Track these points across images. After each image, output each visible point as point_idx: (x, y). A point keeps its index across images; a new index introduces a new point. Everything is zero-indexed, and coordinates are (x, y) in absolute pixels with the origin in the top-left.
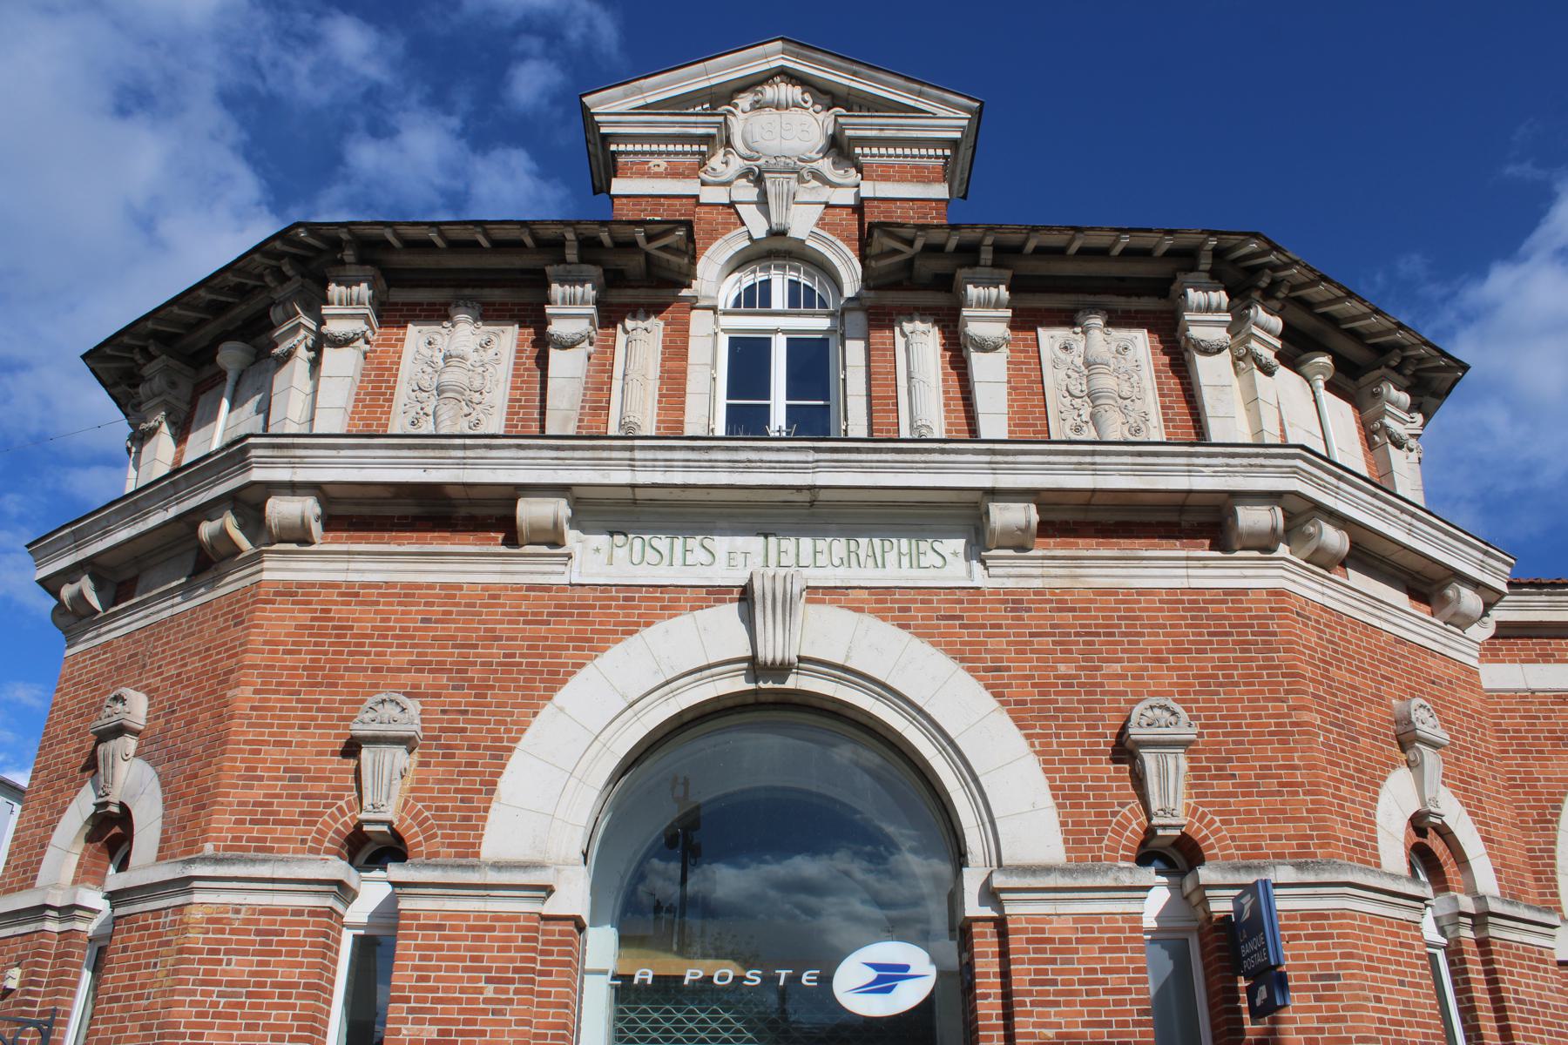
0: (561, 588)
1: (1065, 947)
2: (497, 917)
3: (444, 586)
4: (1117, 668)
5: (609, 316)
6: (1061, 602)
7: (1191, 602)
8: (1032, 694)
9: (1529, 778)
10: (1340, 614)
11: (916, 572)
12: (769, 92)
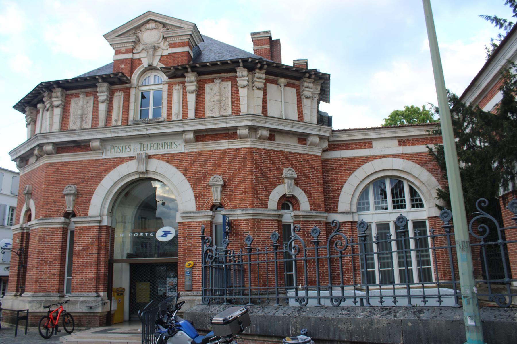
0: (102, 159)
1: (194, 228)
2: (92, 227)
3: (80, 161)
4: (211, 168)
6: (200, 154)
7: (228, 152)
9: (337, 179)
10: (269, 150)
11: (171, 150)
12: (148, 26)
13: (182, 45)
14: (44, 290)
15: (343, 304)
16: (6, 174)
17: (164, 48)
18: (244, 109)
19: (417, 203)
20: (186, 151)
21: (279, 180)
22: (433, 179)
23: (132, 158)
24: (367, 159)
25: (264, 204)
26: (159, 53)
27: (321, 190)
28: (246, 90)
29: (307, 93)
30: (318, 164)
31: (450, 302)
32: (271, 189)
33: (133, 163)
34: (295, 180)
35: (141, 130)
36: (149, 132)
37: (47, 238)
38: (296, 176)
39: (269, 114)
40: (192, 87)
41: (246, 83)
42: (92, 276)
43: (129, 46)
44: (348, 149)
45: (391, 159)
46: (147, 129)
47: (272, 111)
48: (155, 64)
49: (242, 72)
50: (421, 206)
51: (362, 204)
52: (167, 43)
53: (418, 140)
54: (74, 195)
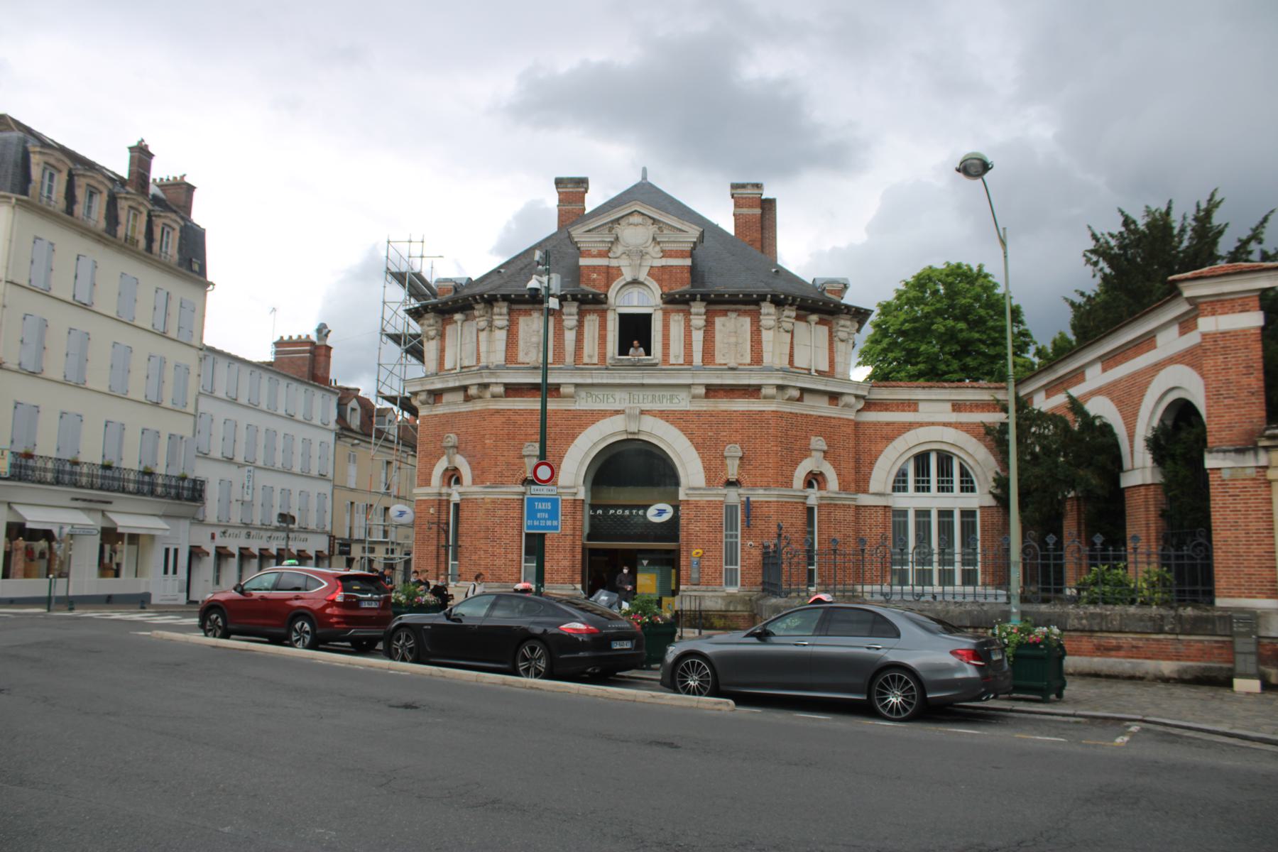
1: (703, 508)
5: (581, 315)
6: (711, 414)
7: (748, 415)
8: (700, 441)
13: (680, 254)
14: (499, 580)
15: (923, 599)
16: (219, 359)
18: (767, 359)
19: (968, 486)
21: (806, 452)
23: (617, 412)
24: (910, 426)
25: (788, 484)
26: (649, 262)
27: (852, 464)
28: (771, 332)
29: (842, 335)
30: (850, 430)
31: (1003, 599)
32: (797, 464)
33: (619, 418)
34: (825, 452)
36: (645, 381)
37: (499, 512)
38: (825, 448)
40: (698, 321)
42: (566, 563)
43: (603, 247)
44: (886, 410)
45: (941, 428)
48: (641, 279)
49: (767, 308)
50: (973, 490)
51: (900, 484)
52: (658, 248)
53: (977, 406)
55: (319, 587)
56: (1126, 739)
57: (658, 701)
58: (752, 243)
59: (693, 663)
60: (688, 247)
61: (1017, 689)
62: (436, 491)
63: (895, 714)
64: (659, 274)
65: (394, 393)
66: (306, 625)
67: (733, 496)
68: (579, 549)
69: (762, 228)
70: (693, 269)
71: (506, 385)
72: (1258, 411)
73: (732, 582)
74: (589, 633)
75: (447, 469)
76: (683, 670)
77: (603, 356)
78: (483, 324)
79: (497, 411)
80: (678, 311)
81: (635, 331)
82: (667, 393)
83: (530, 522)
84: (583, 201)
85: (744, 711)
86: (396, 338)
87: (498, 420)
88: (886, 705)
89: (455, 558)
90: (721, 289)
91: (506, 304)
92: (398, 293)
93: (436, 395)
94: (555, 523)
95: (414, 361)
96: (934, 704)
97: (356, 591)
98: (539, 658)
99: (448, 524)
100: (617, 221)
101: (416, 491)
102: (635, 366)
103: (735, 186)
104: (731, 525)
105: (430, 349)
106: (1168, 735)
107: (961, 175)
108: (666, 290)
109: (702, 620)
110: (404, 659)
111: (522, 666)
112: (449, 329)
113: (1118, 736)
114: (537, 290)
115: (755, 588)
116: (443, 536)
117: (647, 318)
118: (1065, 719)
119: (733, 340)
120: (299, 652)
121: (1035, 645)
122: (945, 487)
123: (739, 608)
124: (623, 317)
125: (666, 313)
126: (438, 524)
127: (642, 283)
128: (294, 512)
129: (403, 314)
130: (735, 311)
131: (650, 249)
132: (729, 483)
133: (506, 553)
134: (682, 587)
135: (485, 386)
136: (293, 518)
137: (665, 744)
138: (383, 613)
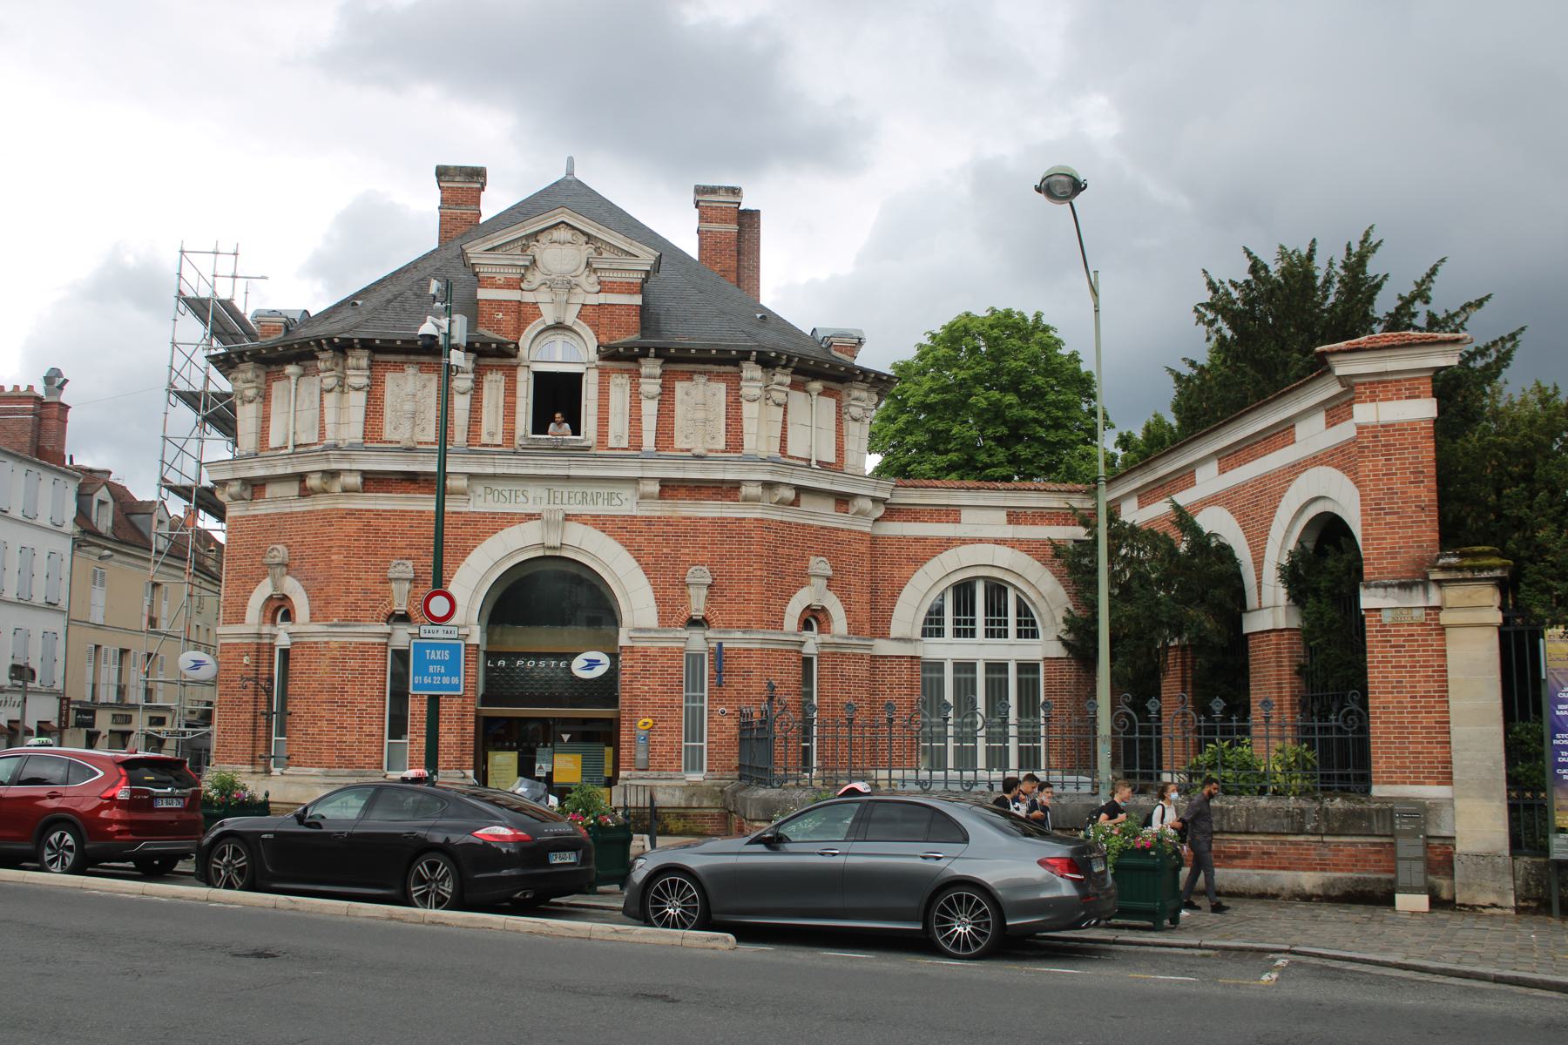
1: (654, 658)
5: (479, 372)
6: (668, 522)
7: (721, 523)
13: (627, 288)
14: (350, 764)
15: (975, 789)
17: (589, 289)
18: (750, 444)
19: (1028, 630)
20: (640, 514)
21: (802, 579)
22: (1061, 591)
23: (530, 517)
24: (948, 543)
25: (777, 624)
26: (579, 298)
27: (867, 597)
28: (756, 405)
29: (855, 411)
31: (1086, 789)
33: (533, 525)
34: (828, 579)
35: (558, 467)
36: (573, 472)
39: (790, 453)
40: (651, 387)
41: (757, 392)
43: (514, 274)
44: (916, 520)
46: (569, 467)
47: (796, 448)
48: (569, 323)
49: (751, 371)
50: (1034, 634)
51: (933, 625)
52: (593, 278)
53: (1042, 516)
54: (411, 581)
55: (89, 778)
56: (1274, 976)
57: (625, 938)
58: (724, 273)
59: (664, 885)
60: (637, 278)
61: (1123, 913)
62: (253, 630)
63: (962, 949)
64: (595, 315)
65: (186, 482)
66: (68, 837)
67: (697, 641)
68: (471, 719)
69: (739, 253)
70: (643, 309)
71: (365, 475)
72: (1429, 533)
73: (695, 766)
74: (518, 841)
75: (270, 598)
76: (658, 892)
77: (510, 434)
78: (330, 381)
79: (351, 513)
80: (622, 371)
81: (558, 398)
82: (605, 490)
83: (418, 679)
84: (478, 204)
85: (750, 950)
86: (191, 399)
87: (352, 526)
88: (949, 938)
89: (282, 732)
90: (685, 341)
91: (366, 353)
92: (193, 329)
93: (256, 486)
94: (455, 680)
95: (215, 433)
96: (1013, 934)
97: (149, 783)
98: (443, 879)
99: (271, 680)
100: (535, 236)
101: (221, 630)
102: (558, 450)
103: (700, 190)
104: (695, 682)
105: (247, 417)
106: (1328, 968)
107: (1042, 196)
108: (604, 339)
109: (653, 821)
110: (229, 885)
111: (416, 891)
112: (277, 388)
113: (1264, 972)
114: (433, 337)
115: (728, 775)
116: (264, 698)
117: (576, 379)
118: (1189, 951)
119: (700, 415)
120: (56, 879)
121: (1144, 851)
122: (996, 630)
123: (705, 804)
124: (540, 377)
125: (604, 374)
126: (256, 680)
127: (569, 329)
128: (35, 664)
129: (203, 362)
130: (704, 373)
131: (582, 280)
132: (693, 623)
133: (361, 725)
134: (622, 774)
135: (333, 474)
136: (33, 672)
137: (656, 996)
138: (186, 816)
